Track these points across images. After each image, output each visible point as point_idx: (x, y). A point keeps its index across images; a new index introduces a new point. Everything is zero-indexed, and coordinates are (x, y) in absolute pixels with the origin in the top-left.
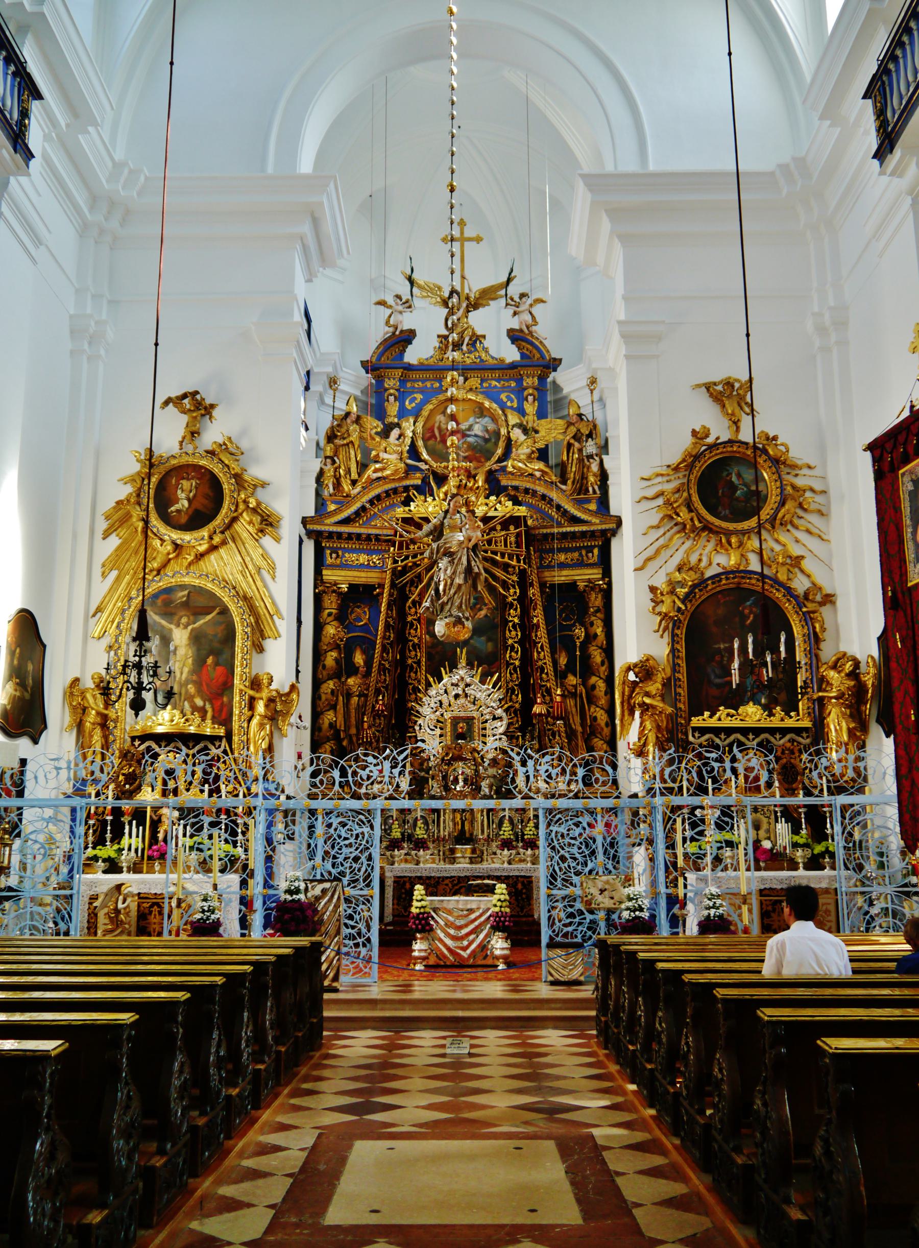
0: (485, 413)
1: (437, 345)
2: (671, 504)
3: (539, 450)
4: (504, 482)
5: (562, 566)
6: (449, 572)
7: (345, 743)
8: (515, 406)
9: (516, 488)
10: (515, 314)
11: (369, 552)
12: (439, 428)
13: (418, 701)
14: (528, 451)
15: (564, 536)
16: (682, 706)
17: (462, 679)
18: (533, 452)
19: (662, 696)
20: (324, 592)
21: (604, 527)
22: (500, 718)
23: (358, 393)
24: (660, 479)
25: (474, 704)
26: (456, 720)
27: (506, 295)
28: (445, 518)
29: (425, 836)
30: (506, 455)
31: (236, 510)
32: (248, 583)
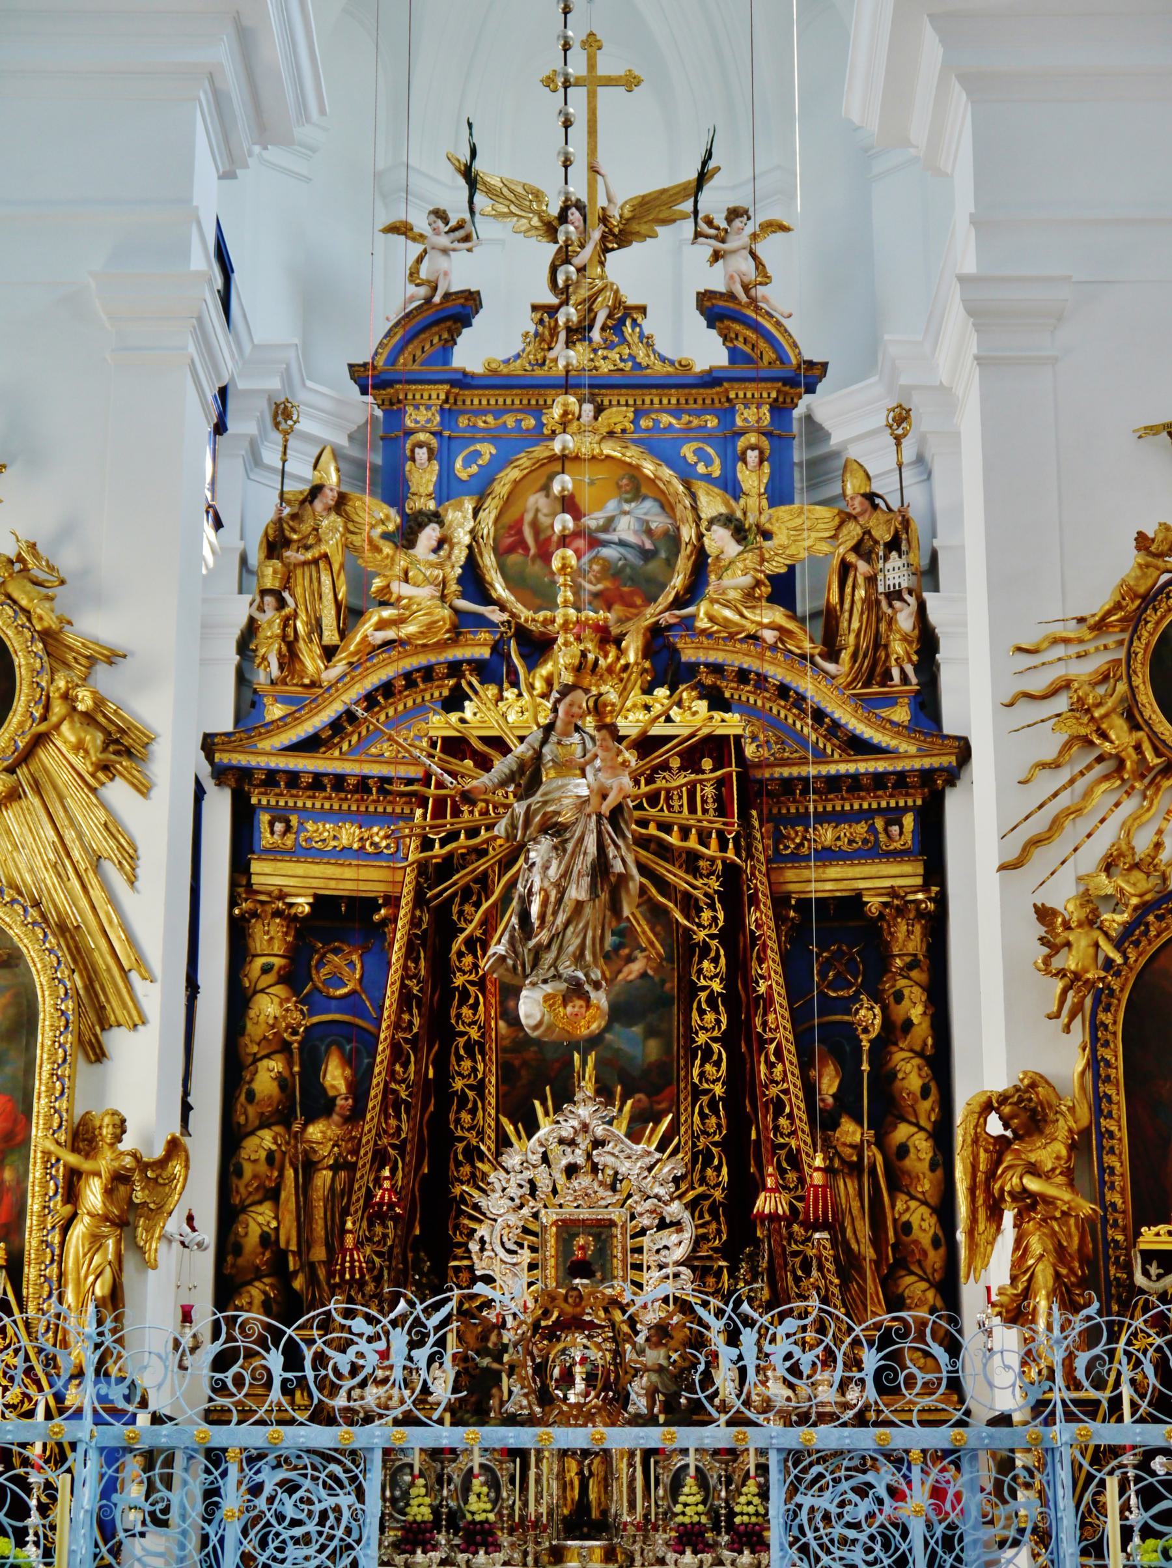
0: (644, 490)
1: (532, 328)
2: (1088, 711)
3: (773, 579)
4: (689, 655)
5: (828, 855)
6: (553, 872)
7: (298, 1284)
8: (717, 473)
9: (717, 669)
10: (717, 256)
11: (364, 820)
12: (535, 524)
13: (478, 1180)
14: (747, 580)
15: (833, 783)
16: (1119, 1201)
17: (585, 1127)
18: (758, 583)
19: (1068, 1173)
20: (254, 914)
21: (927, 763)
22: (677, 1225)
23: (343, 441)
24: (1060, 651)
25: (613, 1189)
26: (568, 1229)
27: (696, 212)
28: (544, 742)
29: (492, 1517)
30: (694, 590)
31: (44, 718)
32: (69, 892)
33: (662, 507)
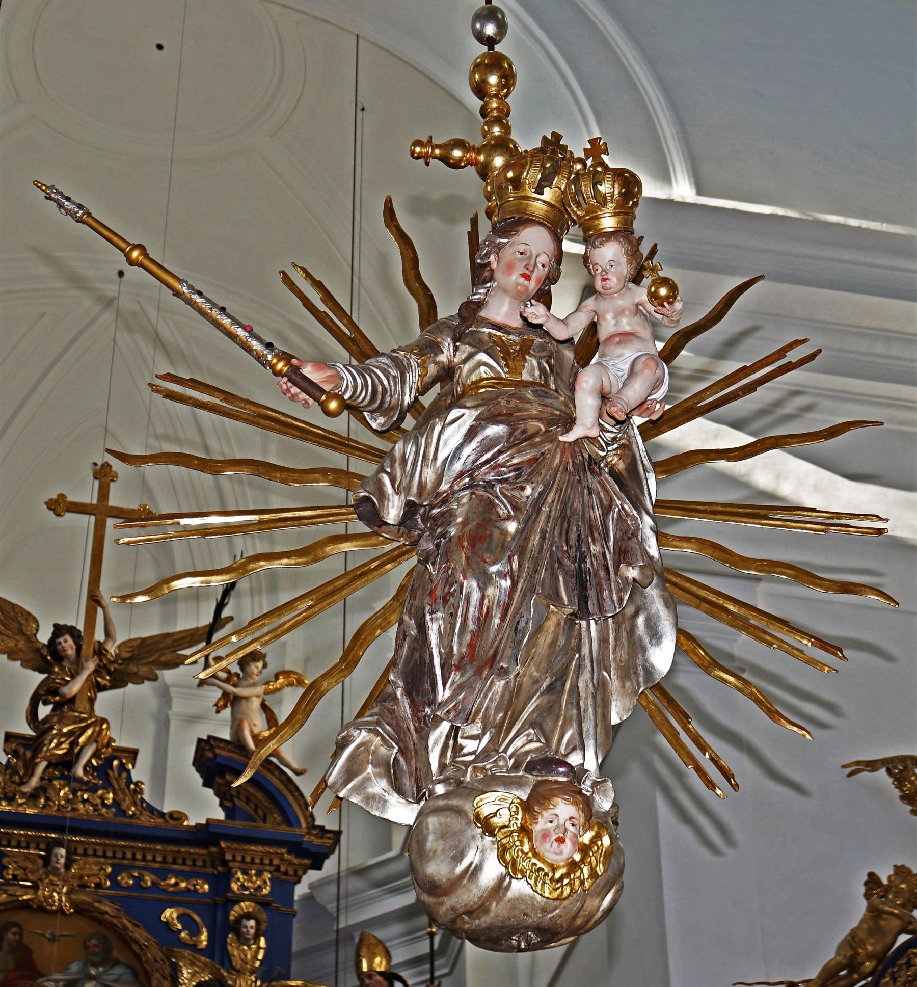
0: (115, 954)
33: (135, 975)
